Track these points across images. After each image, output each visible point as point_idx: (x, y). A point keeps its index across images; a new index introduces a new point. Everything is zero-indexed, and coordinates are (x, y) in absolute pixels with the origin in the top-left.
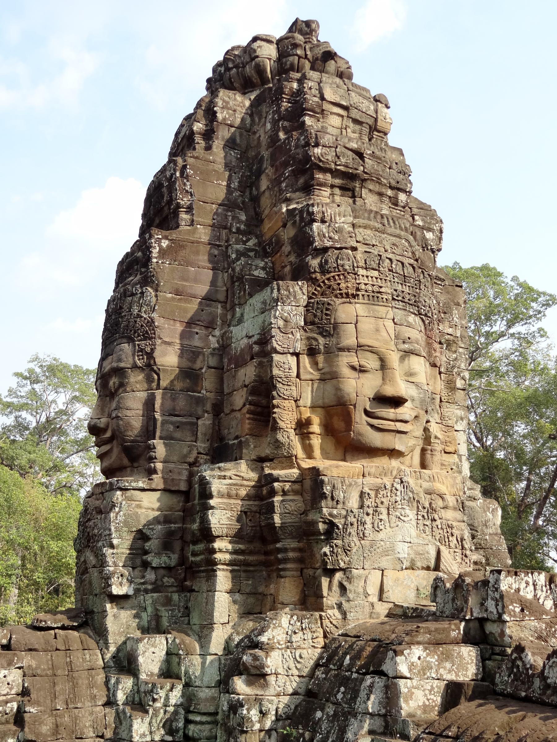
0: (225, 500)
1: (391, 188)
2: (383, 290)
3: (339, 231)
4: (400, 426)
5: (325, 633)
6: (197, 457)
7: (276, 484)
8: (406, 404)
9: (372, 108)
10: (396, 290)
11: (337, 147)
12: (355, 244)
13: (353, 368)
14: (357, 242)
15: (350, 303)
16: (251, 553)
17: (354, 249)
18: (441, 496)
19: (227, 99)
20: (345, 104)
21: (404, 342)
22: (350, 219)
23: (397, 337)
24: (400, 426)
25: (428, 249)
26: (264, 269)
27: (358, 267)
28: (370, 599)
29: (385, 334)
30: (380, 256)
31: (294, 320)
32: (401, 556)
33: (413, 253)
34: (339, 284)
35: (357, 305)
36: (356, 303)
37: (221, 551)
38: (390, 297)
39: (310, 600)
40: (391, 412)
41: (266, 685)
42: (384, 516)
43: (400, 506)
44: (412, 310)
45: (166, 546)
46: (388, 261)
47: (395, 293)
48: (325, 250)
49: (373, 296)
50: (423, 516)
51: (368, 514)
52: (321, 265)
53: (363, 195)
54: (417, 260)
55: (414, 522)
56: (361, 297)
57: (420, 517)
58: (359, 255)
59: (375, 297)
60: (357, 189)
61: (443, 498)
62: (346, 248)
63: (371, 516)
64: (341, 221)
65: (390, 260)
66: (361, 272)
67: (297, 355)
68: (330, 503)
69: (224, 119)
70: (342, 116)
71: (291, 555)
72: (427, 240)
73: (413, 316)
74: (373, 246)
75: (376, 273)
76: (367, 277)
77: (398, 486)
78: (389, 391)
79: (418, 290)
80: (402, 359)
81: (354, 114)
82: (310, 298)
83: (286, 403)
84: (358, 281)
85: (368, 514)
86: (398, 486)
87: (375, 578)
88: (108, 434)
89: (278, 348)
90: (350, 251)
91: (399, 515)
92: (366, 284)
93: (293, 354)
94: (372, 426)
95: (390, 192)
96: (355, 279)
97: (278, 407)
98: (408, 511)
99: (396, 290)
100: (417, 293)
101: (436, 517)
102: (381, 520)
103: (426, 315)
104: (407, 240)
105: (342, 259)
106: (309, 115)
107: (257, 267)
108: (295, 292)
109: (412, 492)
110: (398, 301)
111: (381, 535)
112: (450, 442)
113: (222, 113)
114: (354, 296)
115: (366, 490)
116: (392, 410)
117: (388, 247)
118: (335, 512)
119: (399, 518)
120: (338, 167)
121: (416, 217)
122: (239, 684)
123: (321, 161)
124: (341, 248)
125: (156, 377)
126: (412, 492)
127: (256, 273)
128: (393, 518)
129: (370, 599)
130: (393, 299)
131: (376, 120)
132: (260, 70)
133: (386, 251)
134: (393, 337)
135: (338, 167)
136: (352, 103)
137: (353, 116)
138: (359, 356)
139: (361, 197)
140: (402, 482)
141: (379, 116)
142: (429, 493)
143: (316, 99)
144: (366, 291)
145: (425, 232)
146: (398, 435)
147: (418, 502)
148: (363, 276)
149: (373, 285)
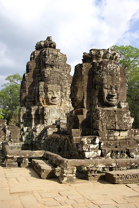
39: (43, 123)
41: (36, 132)
42: (52, 113)
78: (54, 97)
80: (56, 92)
87: (51, 120)
95: (58, 67)
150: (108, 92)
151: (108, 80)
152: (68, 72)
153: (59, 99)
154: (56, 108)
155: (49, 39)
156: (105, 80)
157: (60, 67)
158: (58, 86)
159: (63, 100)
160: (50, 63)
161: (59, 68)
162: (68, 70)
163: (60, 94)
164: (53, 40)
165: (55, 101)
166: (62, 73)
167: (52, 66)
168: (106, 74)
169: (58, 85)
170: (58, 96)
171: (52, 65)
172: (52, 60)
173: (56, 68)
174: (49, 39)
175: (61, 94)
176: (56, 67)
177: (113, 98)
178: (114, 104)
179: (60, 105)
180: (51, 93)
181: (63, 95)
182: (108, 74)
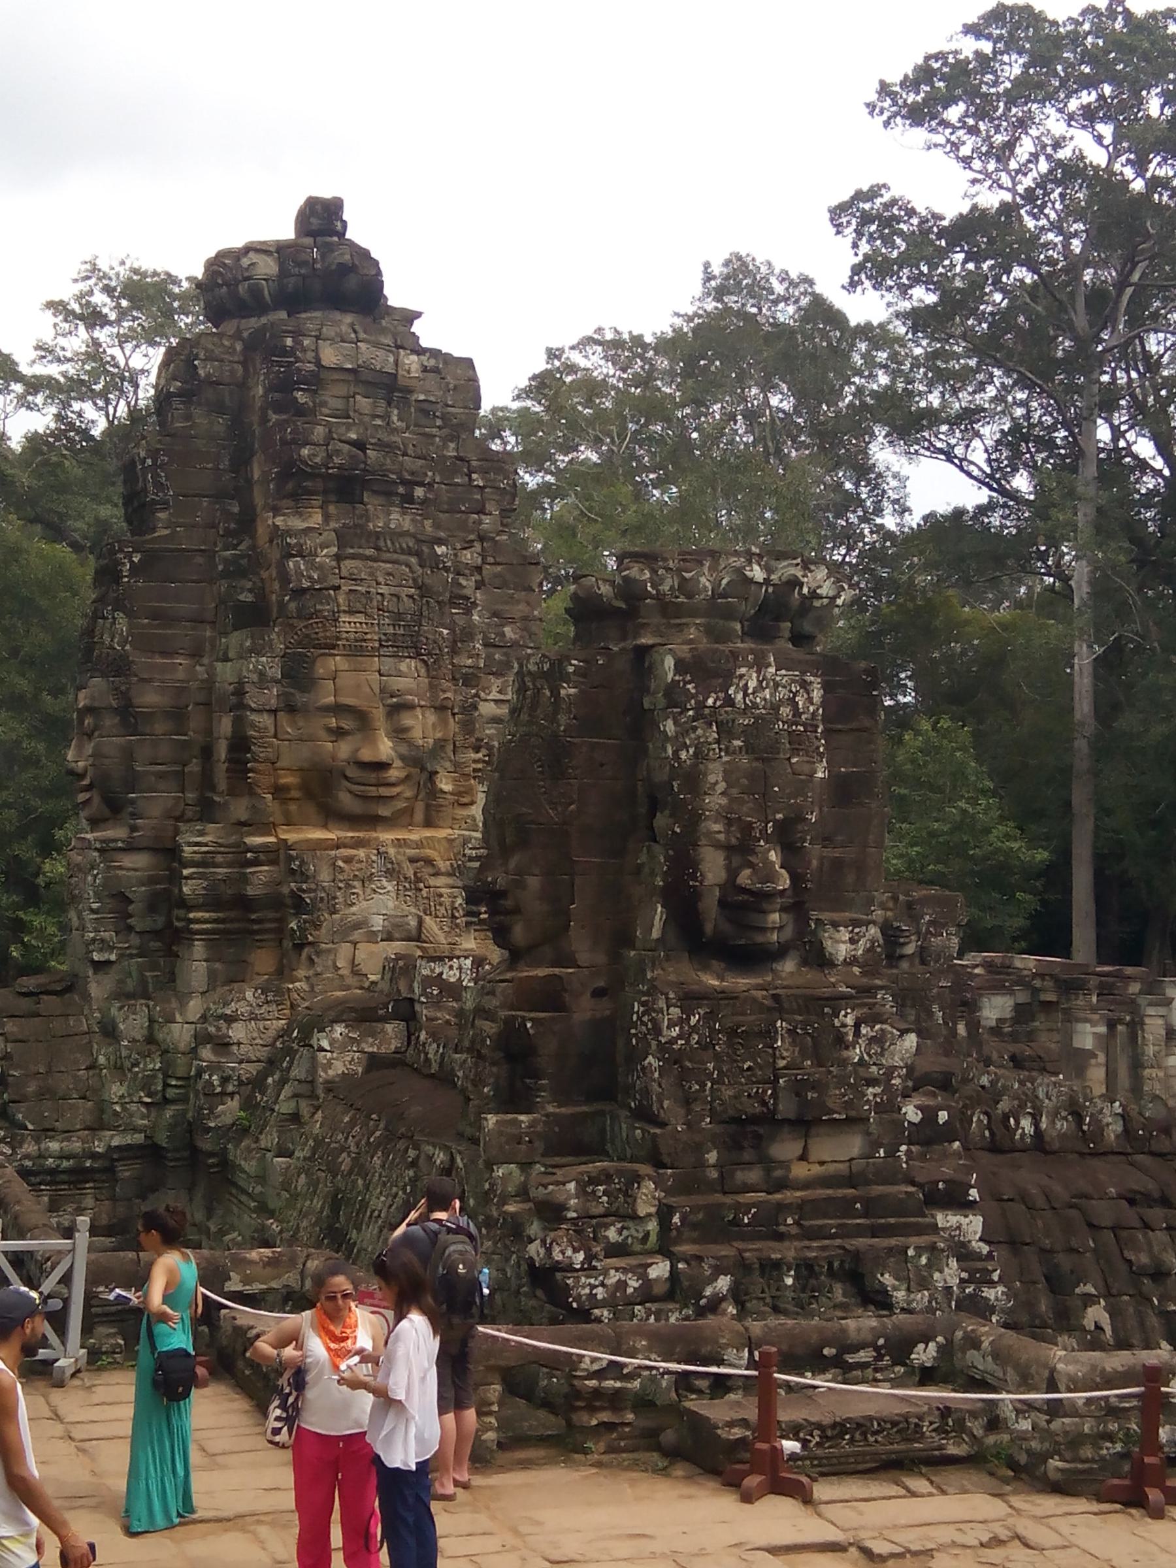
0: (201, 870)
1: (404, 482)
2: (369, 636)
3: (320, 568)
5: (292, 1004)
6: (184, 810)
7: (249, 855)
9: (391, 359)
10: (385, 634)
11: (327, 445)
12: (337, 582)
13: (329, 730)
16: (232, 921)
17: (337, 588)
18: (429, 862)
19: (210, 346)
20: (350, 366)
21: (392, 697)
23: (381, 691)
24: (384, 791)
25: (438, 568)
26: (250, 591)
27: (339, 612)
28: (340, 972)
29: (368, 690)
30: (368, 592)
31: (270, 673)
32: (374, 929)
33: (414, 580)
35: (338, 658)
37: (198, 921)
38: (377, 645)
39: (283, 972)
40: (372, 777)
45: (152, 907)
46: (379, 597)
47: (383, 637)
48: (304, 591)
51: (340, 888)
52: (299, 610)
53: (365, 499)
54: (419, 588)
55: (393, 895)
59: (357, 650)
62: (327, 589)
65: (382, 594)
66: (344, 618)
67: (274, 712)
68: (298, 878)
69: (208, 375)
70: (348, 381)
71: (268, 926)
74: (362, 580)
75: (361, 618)
77: (374, 858)
81: (366, 375)
82: (287, 648)
83: (261, 767)
86: (374, 858)
88: (86, 782)
89: (253, 705)
90: (332, 592)
93: (269, 711)
95: (401, 490)
97: (251, 770)
98: (384, 882)
99: (385, 634)
101: (422, 885)
103: (429, 654)
104: (407, 565)
105: (321, 603)
106: (302, 390)
107: (243, 590)
108: (271, 640)
109: (392, 863)
111: (354, 909)
113: (205, 367)
114: (334, 647)
115: (340, 863)
116: (374, 775)
117: (381, 579)
118: (304, 886)
120: (330, 471)
121: (474, 476)
122: (206, 1053)
124: (320, 589)
125: (133, 720)
126: (392, 863)
127: (242, 597)
128: (368, 891)
129: (340, 972)
130: (381, 645)
131: (395, 375)
132: (256, 292)
134: (377, 691)
135: (330, 471)
136: (360, 362)
137: (363, 378)
141: (401, 372)
142: (412, 860)
143: (311, 367)
147: (399, 872)
152: (487, 520)
155: (321, 218)
157: (419, 492)
161: (409, 498)
162: (489, 507)
164: (360, 229)
165: (384, 791)
166: (440, 550)
173: (380, 500)
174: (321, 218)
180: (346, 724)
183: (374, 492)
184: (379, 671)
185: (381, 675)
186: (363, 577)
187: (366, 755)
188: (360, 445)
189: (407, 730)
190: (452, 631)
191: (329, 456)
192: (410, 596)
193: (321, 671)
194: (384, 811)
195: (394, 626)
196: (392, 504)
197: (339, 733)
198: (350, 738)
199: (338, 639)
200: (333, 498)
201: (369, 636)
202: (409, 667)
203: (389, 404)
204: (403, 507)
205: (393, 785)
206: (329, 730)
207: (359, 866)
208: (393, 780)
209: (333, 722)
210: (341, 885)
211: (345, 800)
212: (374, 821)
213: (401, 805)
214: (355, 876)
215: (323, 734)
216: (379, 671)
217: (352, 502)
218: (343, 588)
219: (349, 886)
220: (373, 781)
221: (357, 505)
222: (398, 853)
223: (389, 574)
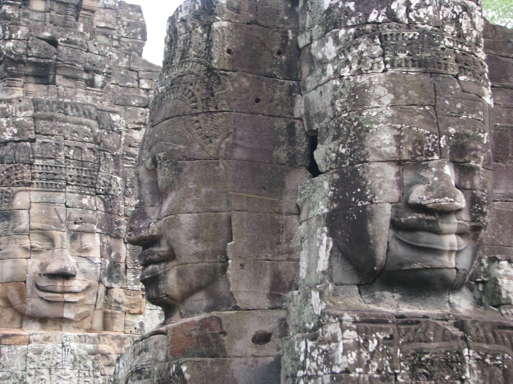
1: (87, 71)
2: (57, 177)
4: (67, 297)
8: (77, 277)
10: (71, 176)
12: (32, 136)
13: (26, 249)
14: (36, 133)
15: (26, 191)
17: (33, 141)
18: (105, 355)
21: (75, 223)
22: (31, 113)
24: (67, 297)
27: (33, 158)
34: (16, 174)
36: (30, 191)
38: (64, 183)
40: (59, 285)
43: (61, 367)
44: (88, 192)
47: (69, 178)
49: (47, 184)
50: (85, 374)
51: (30, 375)
53: (58, 82)
56: (35, 185)
57: (81, 375)
58: (36, 146)
60: (51, 77)
61: (108, 357)
63: (33, 377)
64: (22, 115)
66: (37, 162)
72: (113, 122)
73: (89, 197)
74: (52, 135)
75: (52, 162)
76: (42, 166)
77: (60, 350)
79: (96, 173)
84: (33, 171)
85: (30, 375)
86: (60, 350)
90: (28, 144)
91: (58, 373)
92: (40, 173)
94: (42, 298)
95: (85, 76)
96: (31, 169)
99: (71, 176)
100: (94, 175)
101: (98, 374)
102: (42, 379)
104: (89, 126)
110: (73, 185)
112: (135, 304)
114: (30, 184)
117: (68, 136)
119: (59, 377)
120: (30, 59)
123: (12, 54)
124: (19, 141)
128: (54, 377)
133: (65, 139)
135: (30, 59)
138: (32, 238)
139: (54, 83)
140: (63, 346)
144: (40, 179)
145: (111, 115)
146: (66, 305)
148: (38, 165)
149: (47, 174)
150: (400, 184)
151: (397, 96)
153: (94, 282)
154: (74, 345)
156: (378, 99)
157: (99, 79)
158: (85, 201)
159: (117, 293)
160: (35, 51)
161: (91, 83)
163: (96, 254)
167: (43, 73)
168: (383, 55)
169: (83, 195)
170: (85, 265)
171: (47, 66)
172: (47, 34)
173: (70, 83)
175: (107, 251)
176: (75, 79)
177: (444, 226)
178: (452, 275)
179: (98, 322)
181: (118, 256)
182: (402, 56)
183: (66, 77)
184: (65, 204)
185: (67, 207)
186: (54, 133)
187: (54, 267)
188: (53, 42)
189: (87, 250)
190: (124, 179)
191: (29, 48)
192: (91, 149)
193: (19, 203)
194: (68, 314)
195: (78, 169)
196: (77, 86)
197: (32, 250)
198: (42, 255)
199: (33, 178)
200: (32, 79)
201: (57, 177)
202: (89, 202)
203: (77, 19)
204: (86, 89)
205: (76, 293)
206: (26, 249)
207: (46, 356)
208: (75, 289)
209: (27, 243)
210: (33, 372)
211: (35, 304)
212: (61, 321)
213: (82, 310)
214: (44, 365)
215: (20, 253)
216: (65, 204)
217: (47, 84)
218: (38, 140)
219: (38, 373)
220: (59, 289)
221: (51, 86)
222: (80, 347)
223: (75, 132)
